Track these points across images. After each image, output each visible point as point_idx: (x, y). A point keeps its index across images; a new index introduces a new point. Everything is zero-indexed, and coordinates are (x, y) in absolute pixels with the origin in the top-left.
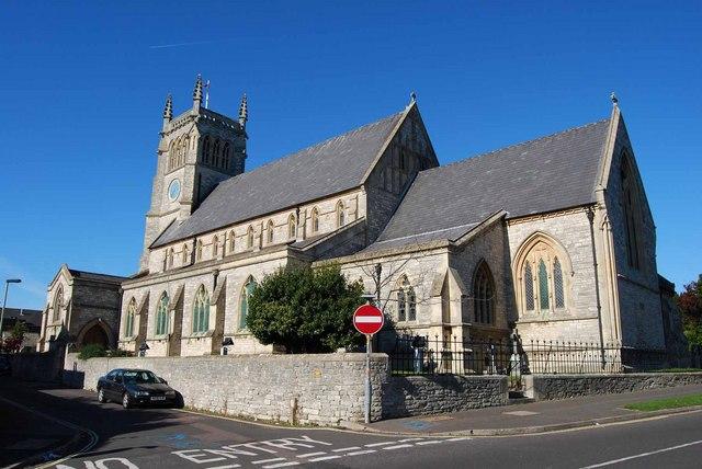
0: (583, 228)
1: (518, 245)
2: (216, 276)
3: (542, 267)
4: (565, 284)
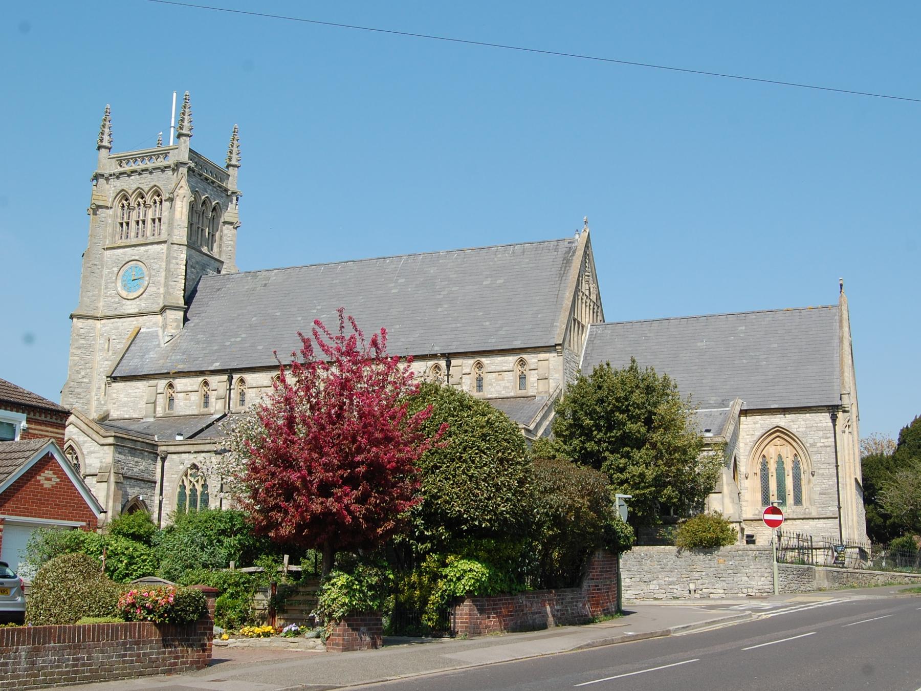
0: (825, 429)
3: (780, 462)
4: (804, 482)
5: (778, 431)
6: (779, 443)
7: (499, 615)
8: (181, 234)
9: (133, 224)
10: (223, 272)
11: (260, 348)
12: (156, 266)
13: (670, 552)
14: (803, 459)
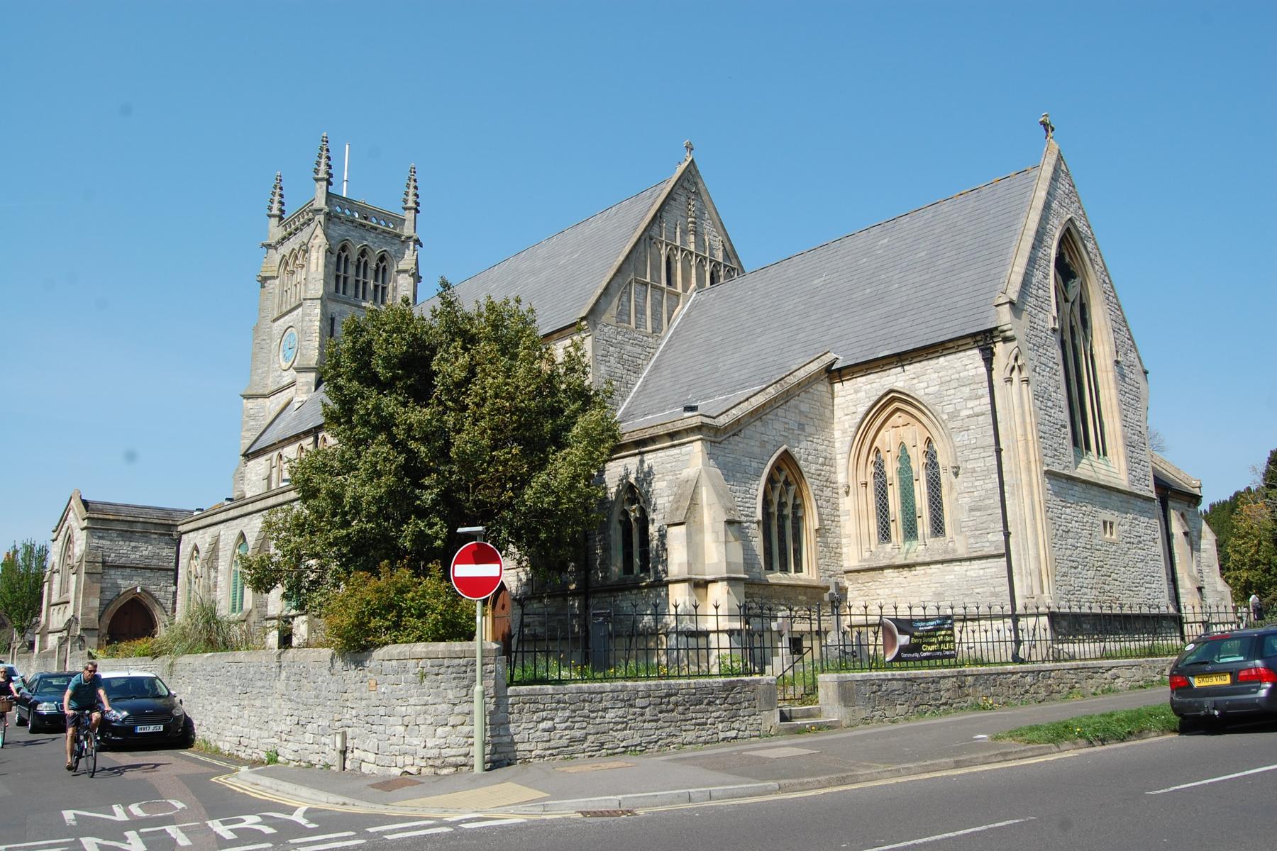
1: (858, 420)
3: (904, 458)
4: (944, 490)
6: (900, 421)
8: (317, 289)
14: (941, 445)
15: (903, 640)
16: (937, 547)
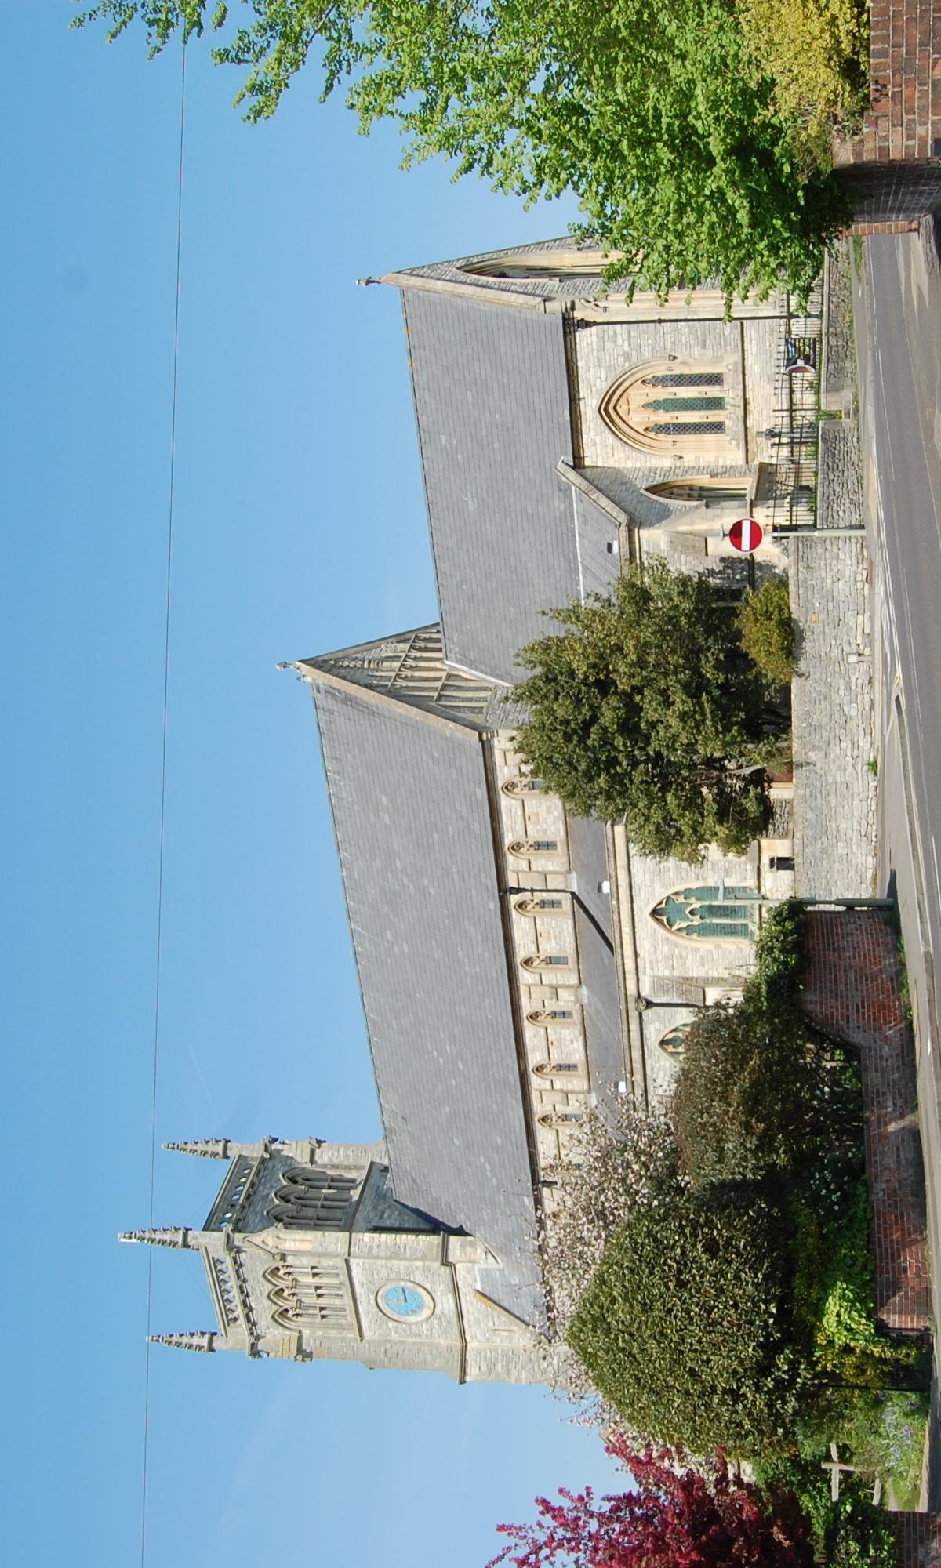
1: (619, 444)
2: (649, 1004)
3: (656, 405)
4: (686, 371)
5: (606, 410)
6: (625, 407)
7: (903, 1245)
8: (335, 1240)
9: (322, 1302)
10: (386, 1162)
11: (499, 1141)
12: (384, 1273)
13: (802, 693)
15: (800, 363)
16: (731, 379)
